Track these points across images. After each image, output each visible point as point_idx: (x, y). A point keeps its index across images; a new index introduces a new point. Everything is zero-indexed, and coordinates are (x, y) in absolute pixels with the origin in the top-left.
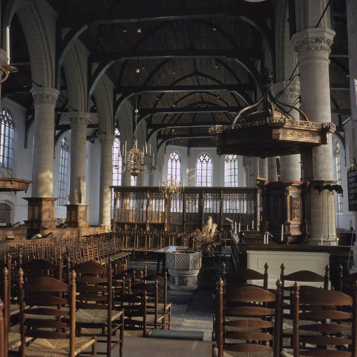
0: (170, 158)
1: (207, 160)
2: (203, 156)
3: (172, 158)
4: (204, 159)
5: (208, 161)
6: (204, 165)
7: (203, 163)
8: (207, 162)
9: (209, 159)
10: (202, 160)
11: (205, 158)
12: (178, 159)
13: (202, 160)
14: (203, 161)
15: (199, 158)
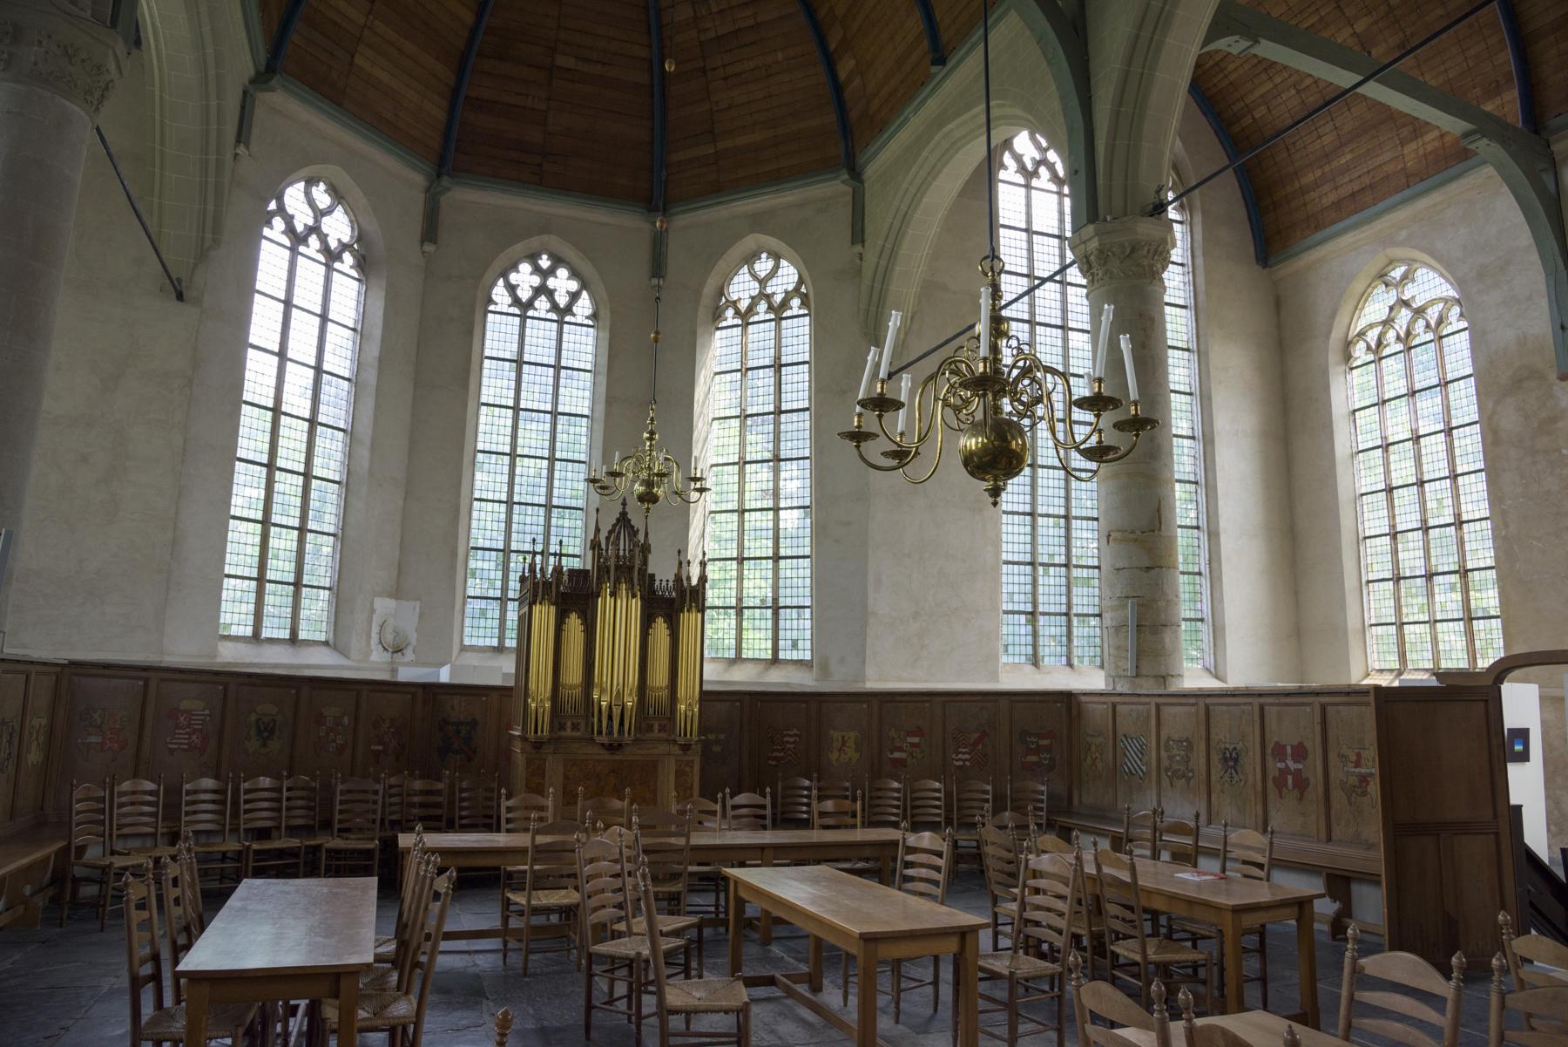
0: (281, 210)
1: (562, 301)
2: (537, 270)
3: (303, 219)
4: (541, 290)
5: (568, 310)
6: (540, 336)
7: (530, 313)
8: (562, 313)
9: (574, 297)
10: (524, 294)
11: (551, 283)
12: (344, 247)
13: (524, 294)
14: (530, 304)
15: (505, 275)
